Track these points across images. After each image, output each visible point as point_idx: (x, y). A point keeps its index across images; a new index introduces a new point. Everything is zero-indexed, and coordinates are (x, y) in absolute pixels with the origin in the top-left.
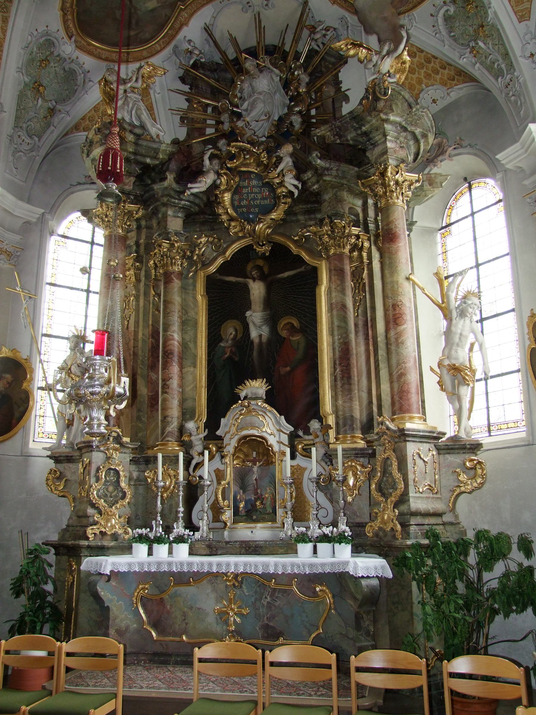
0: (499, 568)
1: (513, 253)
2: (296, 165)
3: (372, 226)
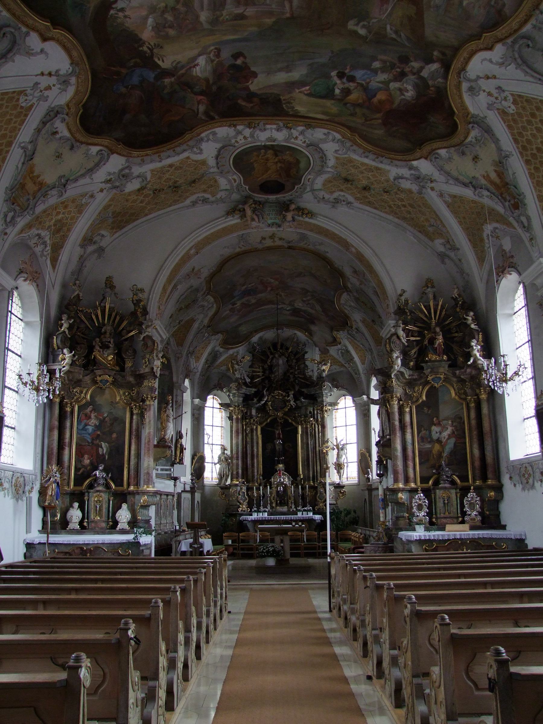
0: (349, 516)
1: (357, 425)
2: (294, 397)
3: (316, 417)
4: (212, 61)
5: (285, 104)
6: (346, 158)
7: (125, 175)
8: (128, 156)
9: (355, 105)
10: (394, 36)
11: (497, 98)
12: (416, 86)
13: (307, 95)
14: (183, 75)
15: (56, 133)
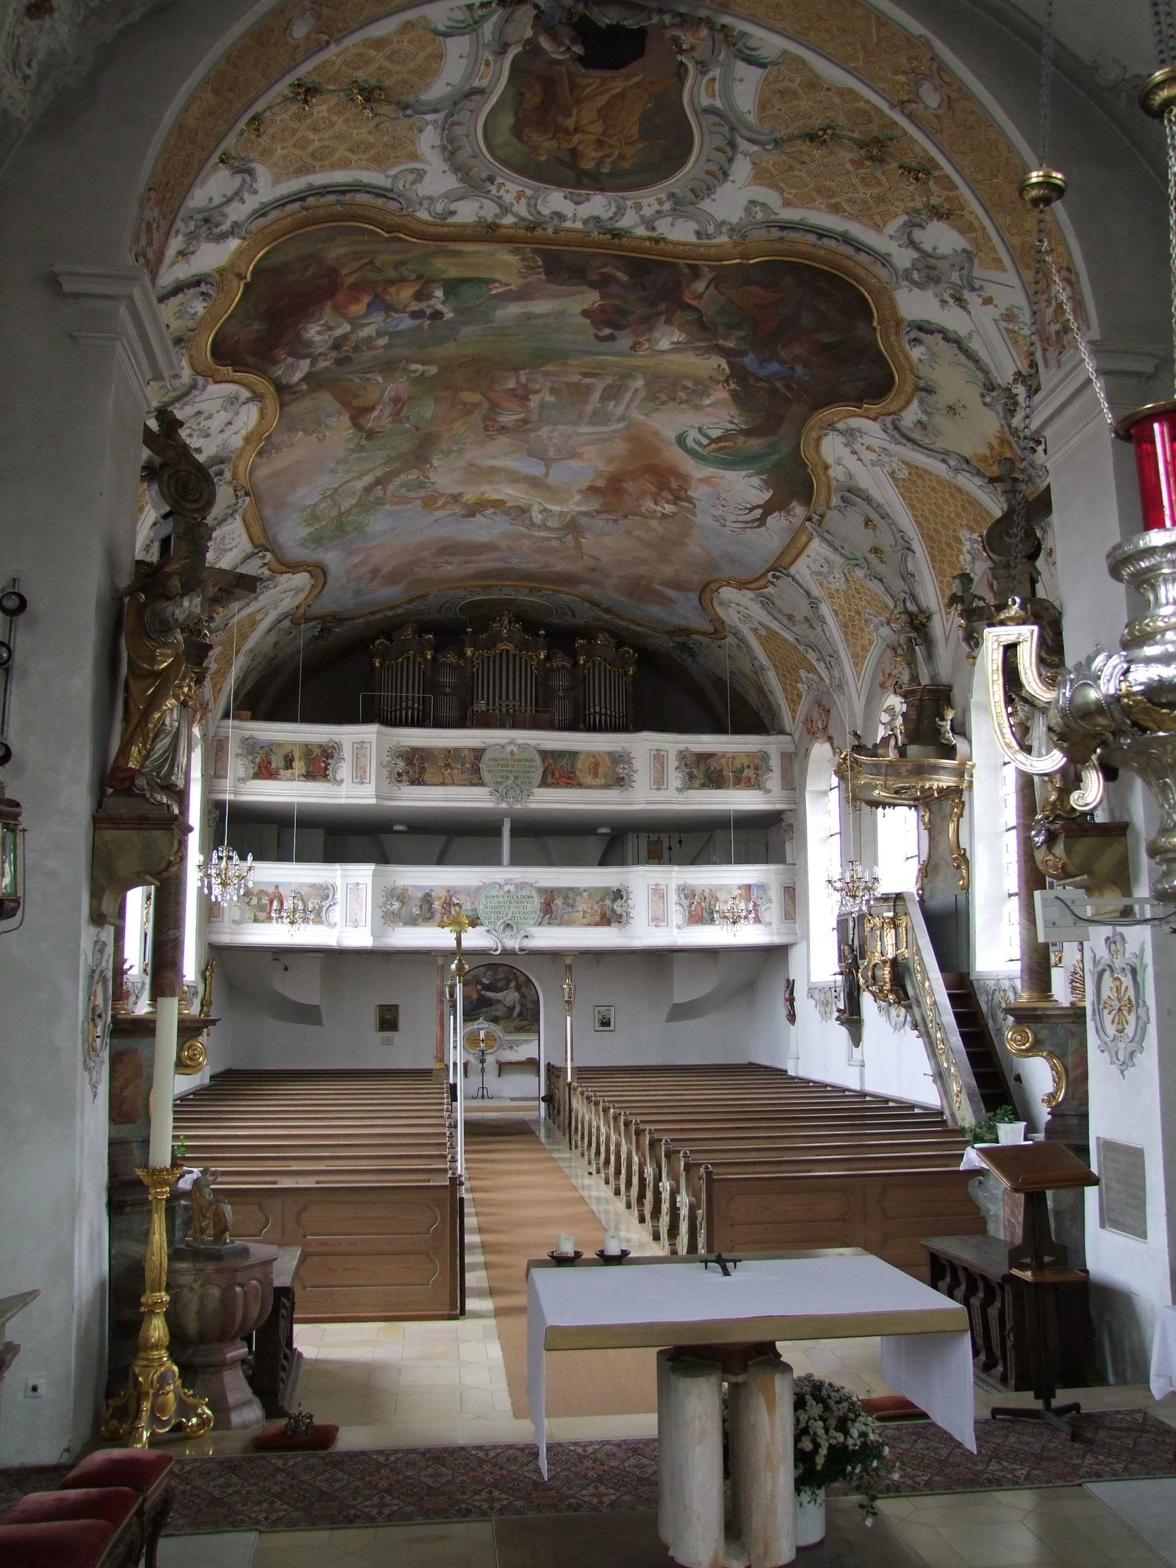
4: (649, 340)
5: (539, 267)
6: (393, 165)
7: (928, 272)
8: (883, 293)
9: (402, 280)
10: (368, 376)
11: (199, 424)
12: (309, 344)
13: (495, 281)
14: (701, 340)
15: (919, 422)
